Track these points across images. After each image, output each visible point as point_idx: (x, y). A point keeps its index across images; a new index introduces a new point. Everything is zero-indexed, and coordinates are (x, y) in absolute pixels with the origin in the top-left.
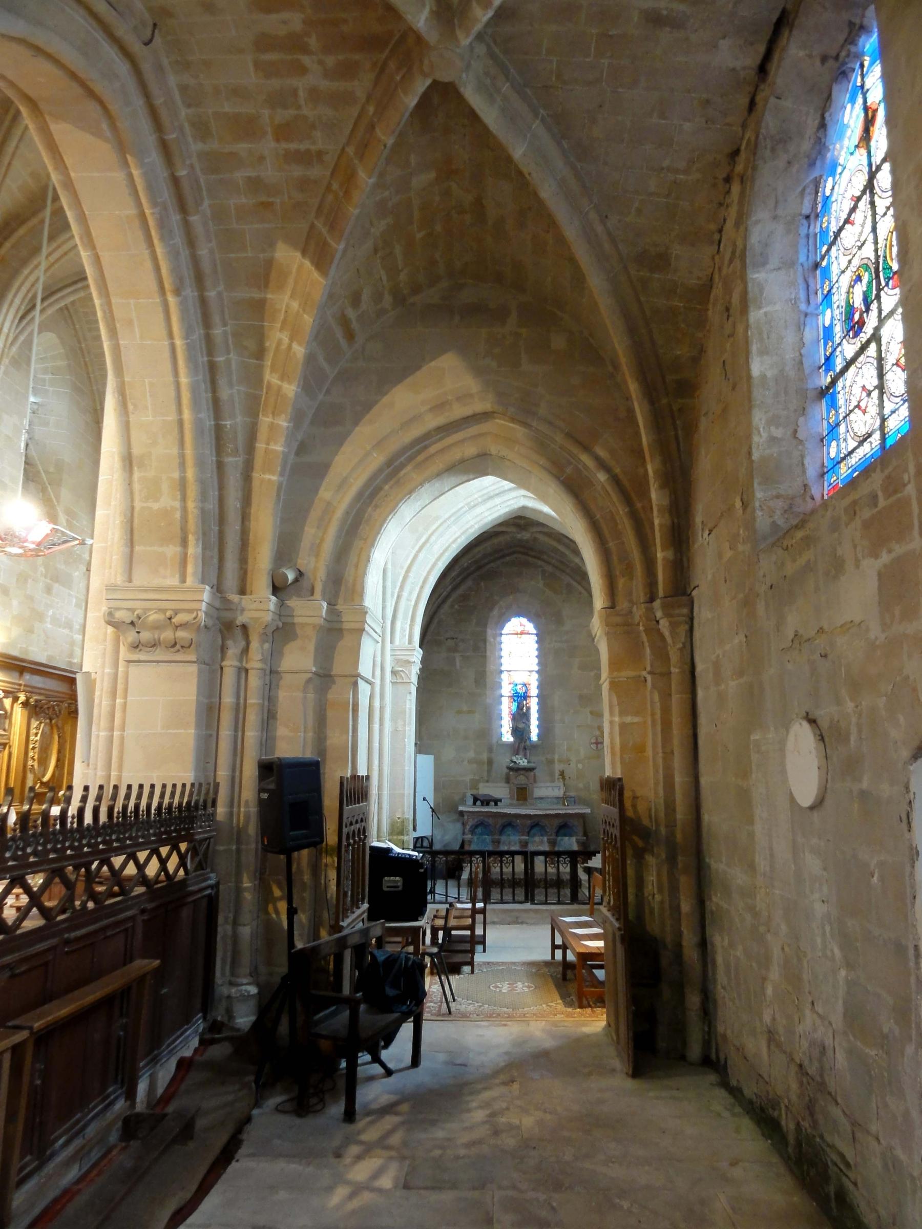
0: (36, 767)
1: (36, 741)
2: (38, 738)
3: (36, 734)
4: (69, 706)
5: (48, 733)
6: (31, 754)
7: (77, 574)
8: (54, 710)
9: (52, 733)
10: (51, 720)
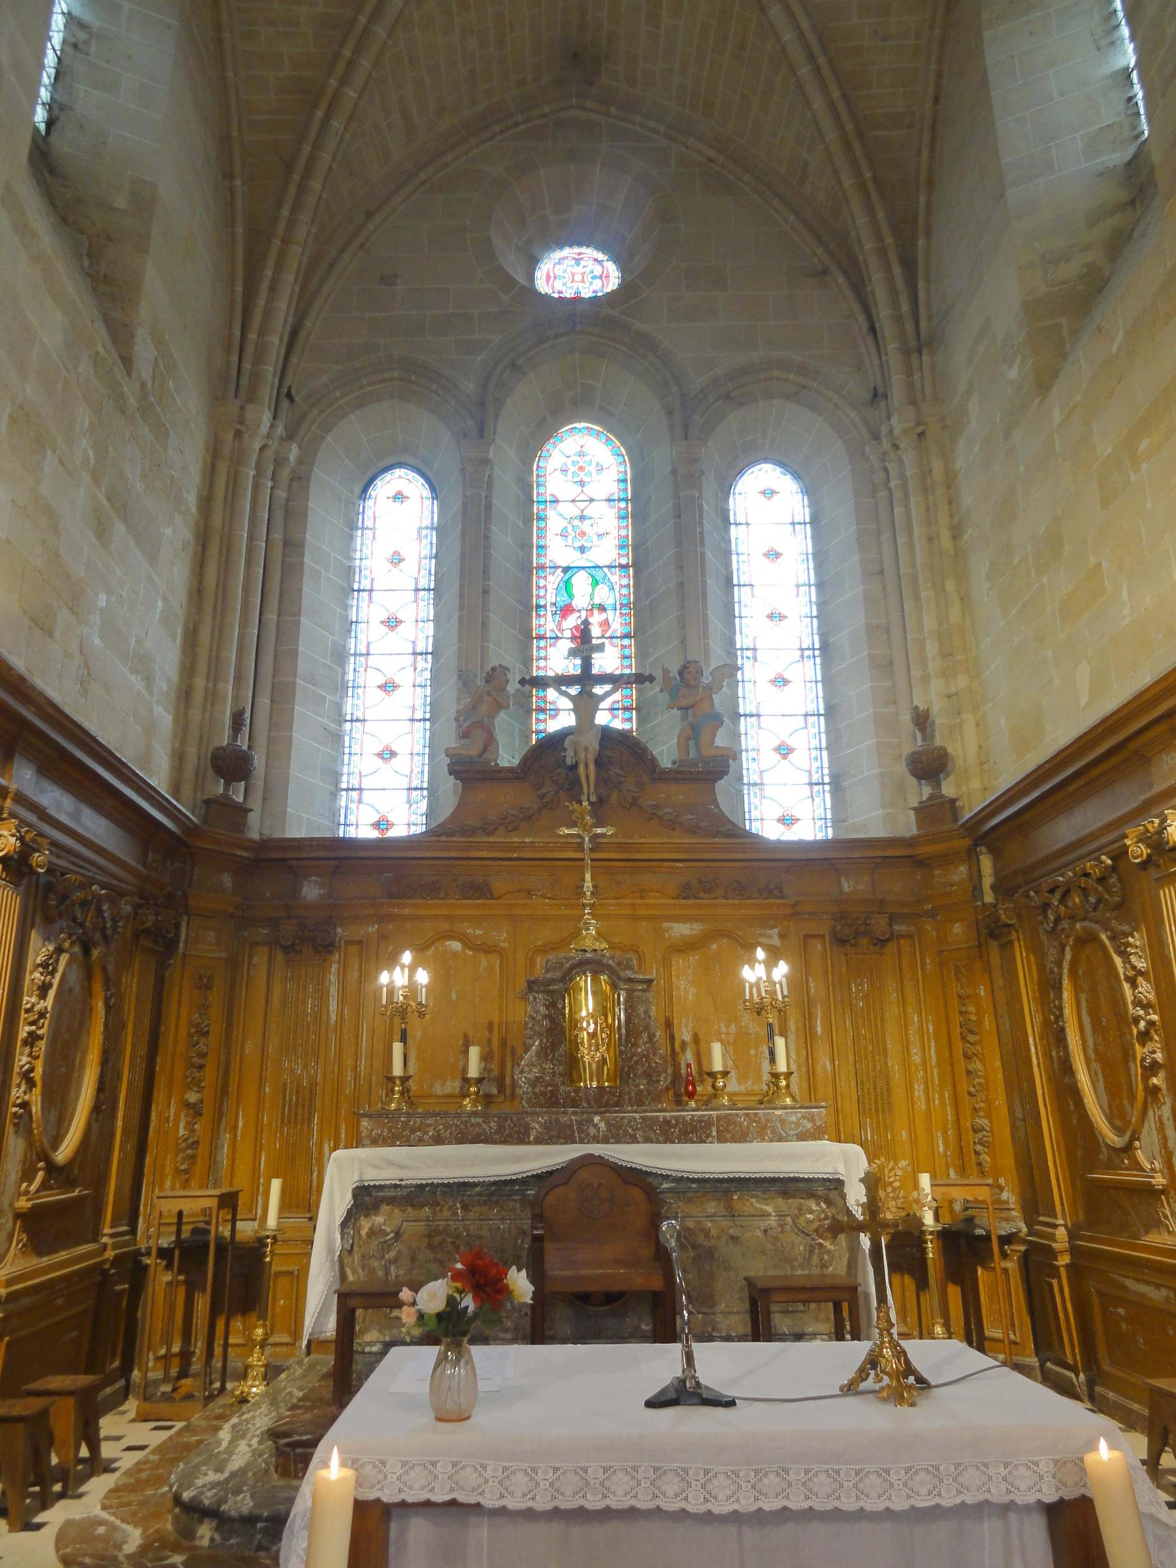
0: (36, 1109)
1: (42, 1015)
2: (49, 1002)
3: (44, 989)
4: (136, 914)
5: (77, 989)
7: (168, 531)
8: (100, 911)
9: (89, 993)
10: (86, 952)
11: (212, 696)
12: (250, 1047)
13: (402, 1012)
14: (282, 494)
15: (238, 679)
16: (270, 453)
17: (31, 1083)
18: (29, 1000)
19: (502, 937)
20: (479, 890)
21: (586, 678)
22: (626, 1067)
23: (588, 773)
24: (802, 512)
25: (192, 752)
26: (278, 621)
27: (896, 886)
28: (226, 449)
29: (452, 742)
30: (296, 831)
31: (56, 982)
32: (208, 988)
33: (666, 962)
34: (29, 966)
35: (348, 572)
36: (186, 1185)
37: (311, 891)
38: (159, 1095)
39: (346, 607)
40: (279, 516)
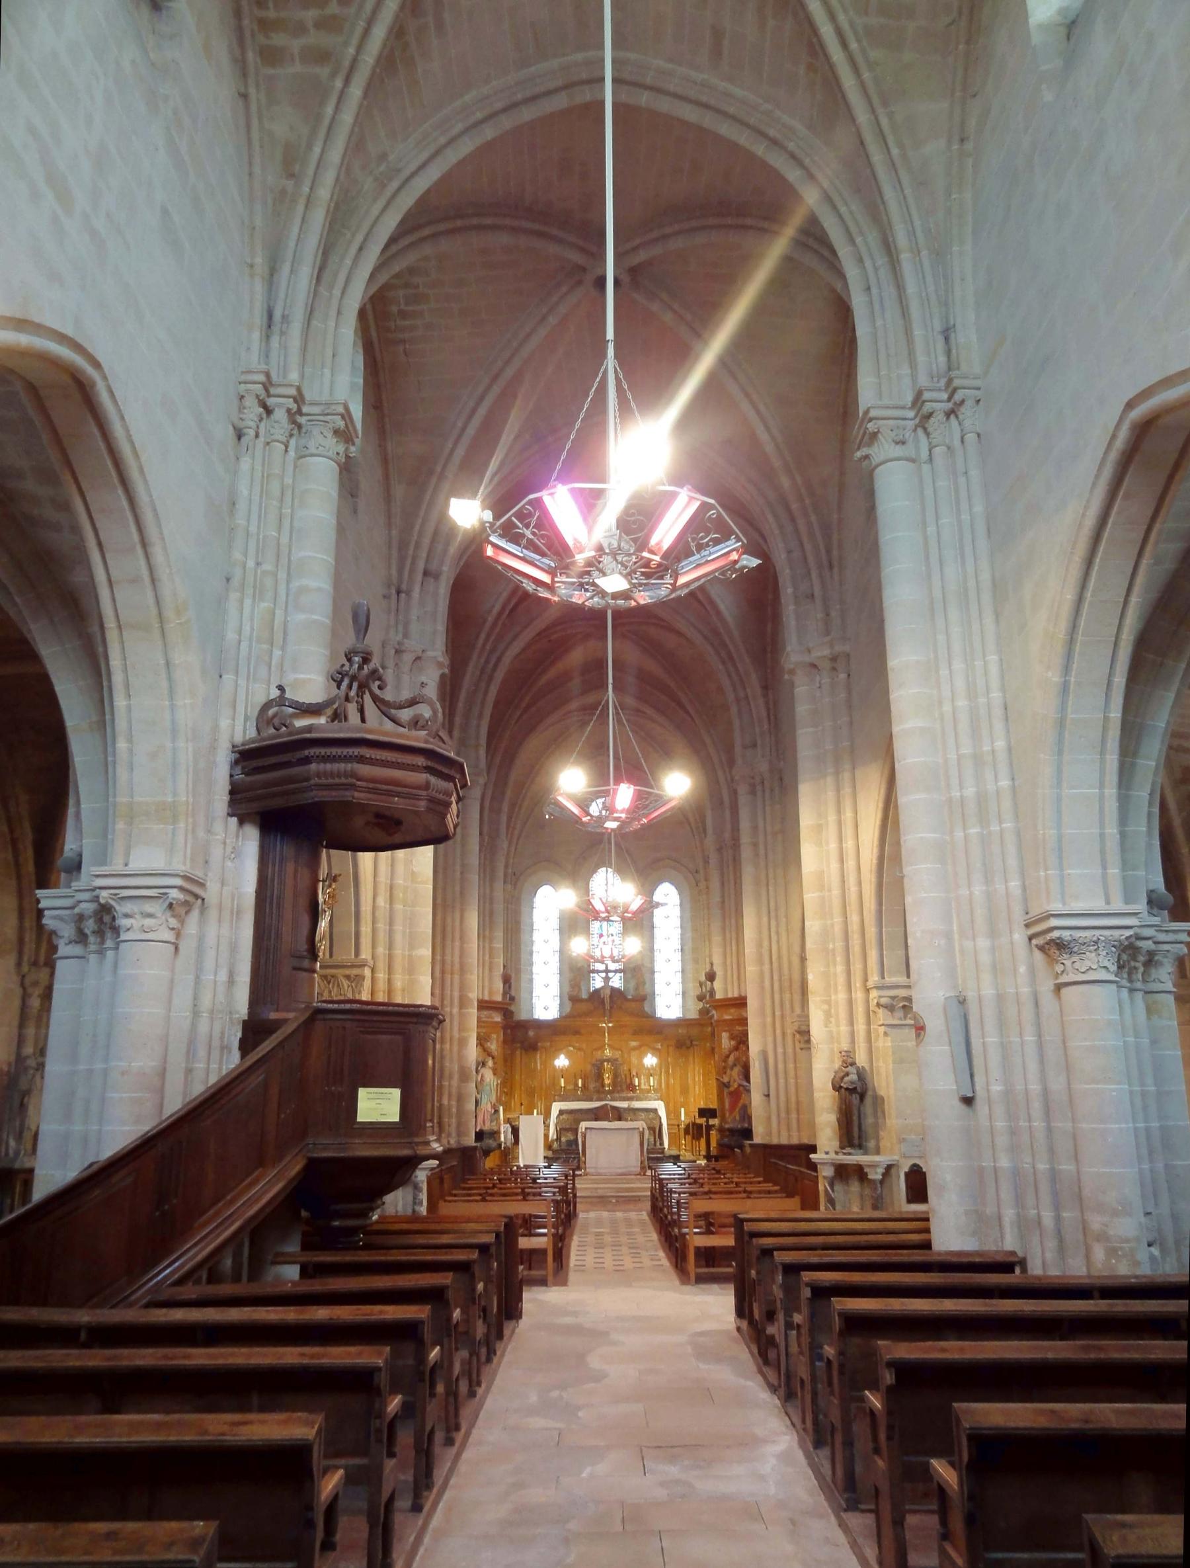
12: (517, 1077)
13: (562, 1070)
19: (584, 1046)
20: (577, 1032)
21: (607, 971)
22: (615, 1083)
23: (607, 1001)
24: (678, 902)
27: (695, 1031)
29: (567, 989)
30: (523, 1016)
33: (629, 1053)
35: (532, 925)
37: (531, 1033)
39: (531, 936)
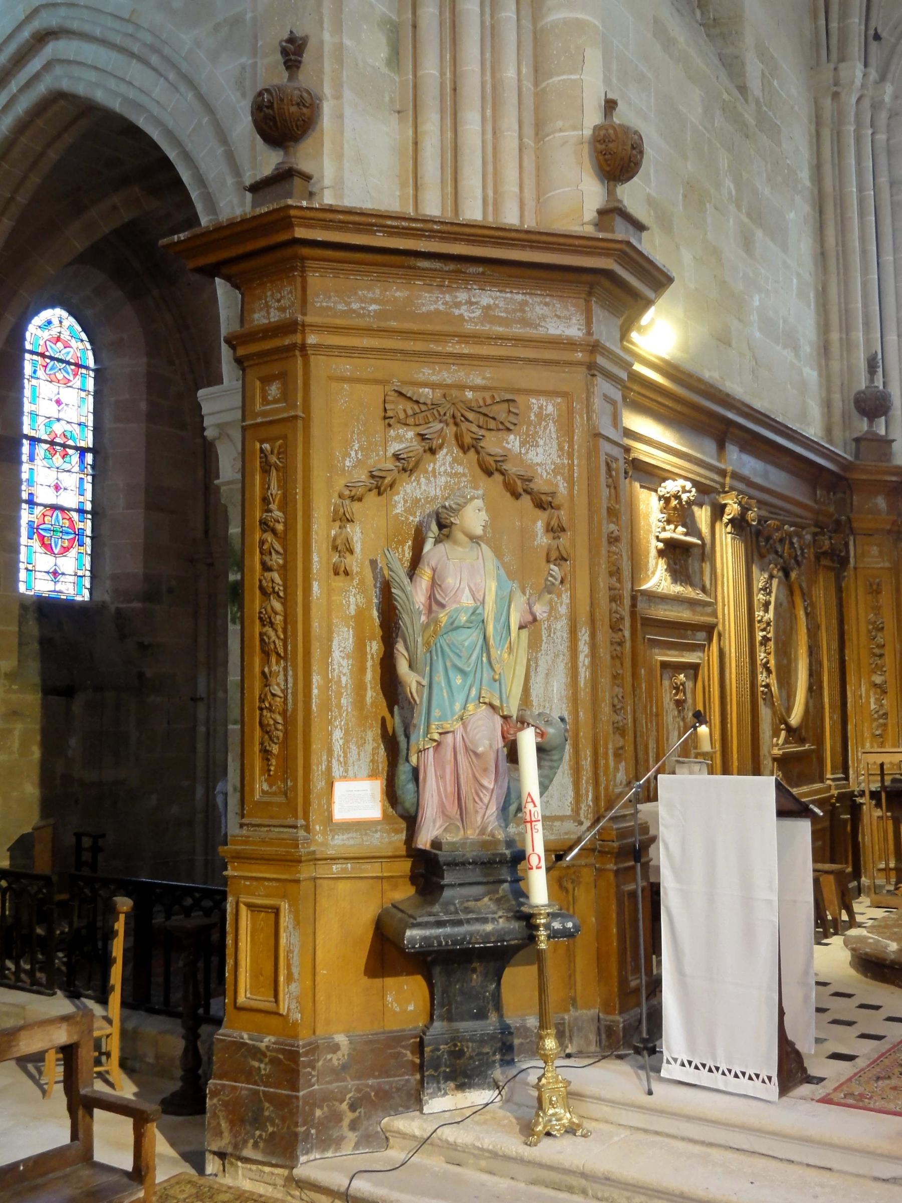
0: (774, 689)
1: (768, 624)
2: (771, 615)
3: (766, 605)
4: (815, 541)
6: (761, 655)
7: (792, 215)
8: (792, 544)
9: (793, 604)
10: (787, 575)
11: (848, 345)
14: (882, 137)
15: (867, 324)
16: (866, 103)
17: (769, 671)
18: (759, 614)
25: (837, 397)
26: (895, 259)
28: (827, 114)
31: (773, 600)
32: (878, 592)
34: (755, 590)
36: (882, 745)
38: (851, 678)
40: (883, 160)
